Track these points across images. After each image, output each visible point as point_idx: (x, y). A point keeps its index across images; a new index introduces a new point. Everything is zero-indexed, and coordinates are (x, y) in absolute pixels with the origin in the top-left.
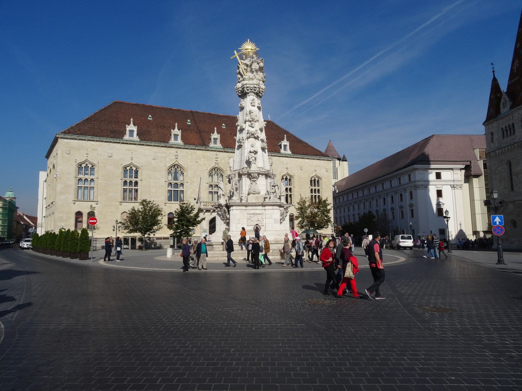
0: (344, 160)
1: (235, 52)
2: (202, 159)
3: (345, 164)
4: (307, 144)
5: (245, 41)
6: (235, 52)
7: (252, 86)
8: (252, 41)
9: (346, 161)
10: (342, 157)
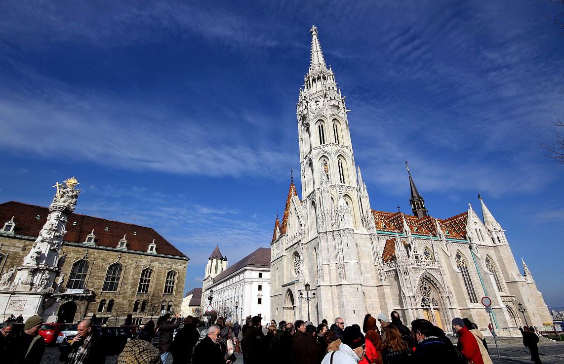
0: (226, 259)
1: (57, 183)
2: (72, 253)
3: (224, 262)
4: (173, 247)
5: (71, 177)
6: (57, 183)
7: (59, 206)
8: (75, 178)
9: (227, 260)
10: (224, 258)
